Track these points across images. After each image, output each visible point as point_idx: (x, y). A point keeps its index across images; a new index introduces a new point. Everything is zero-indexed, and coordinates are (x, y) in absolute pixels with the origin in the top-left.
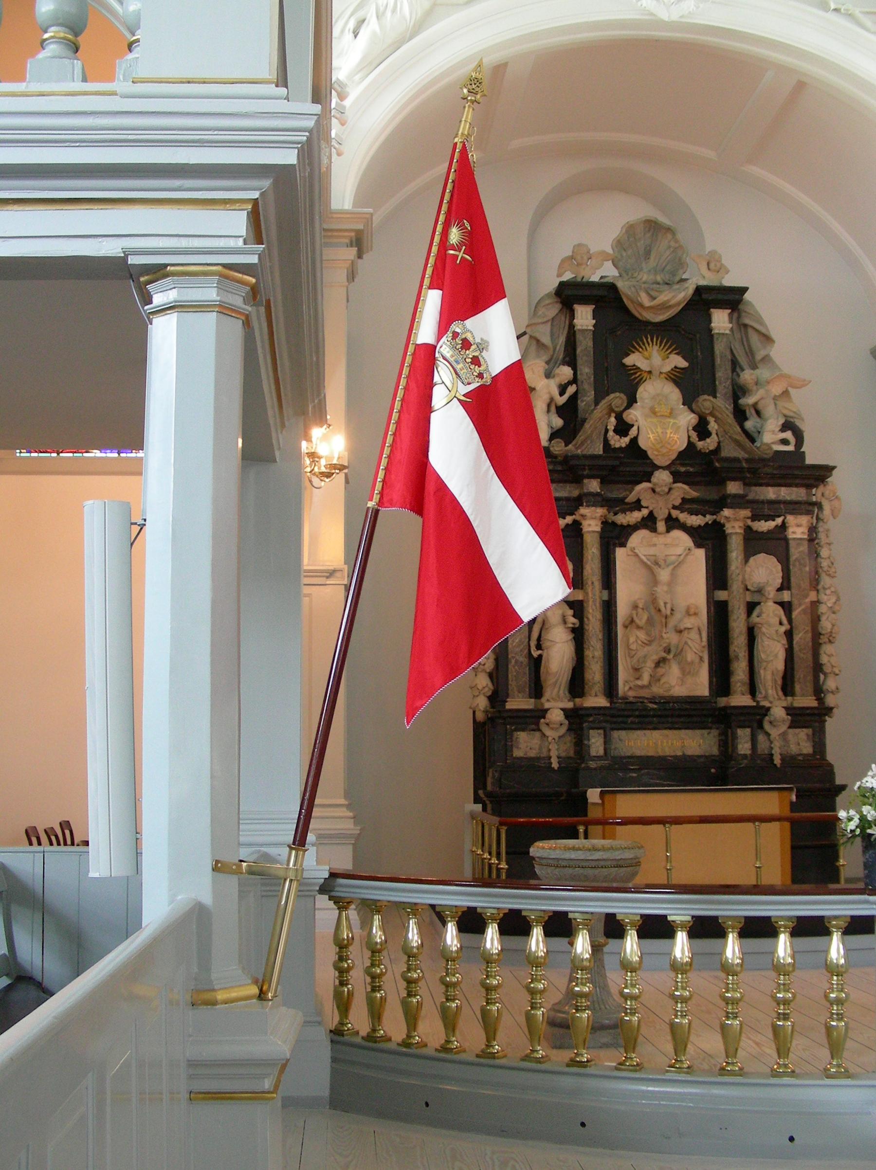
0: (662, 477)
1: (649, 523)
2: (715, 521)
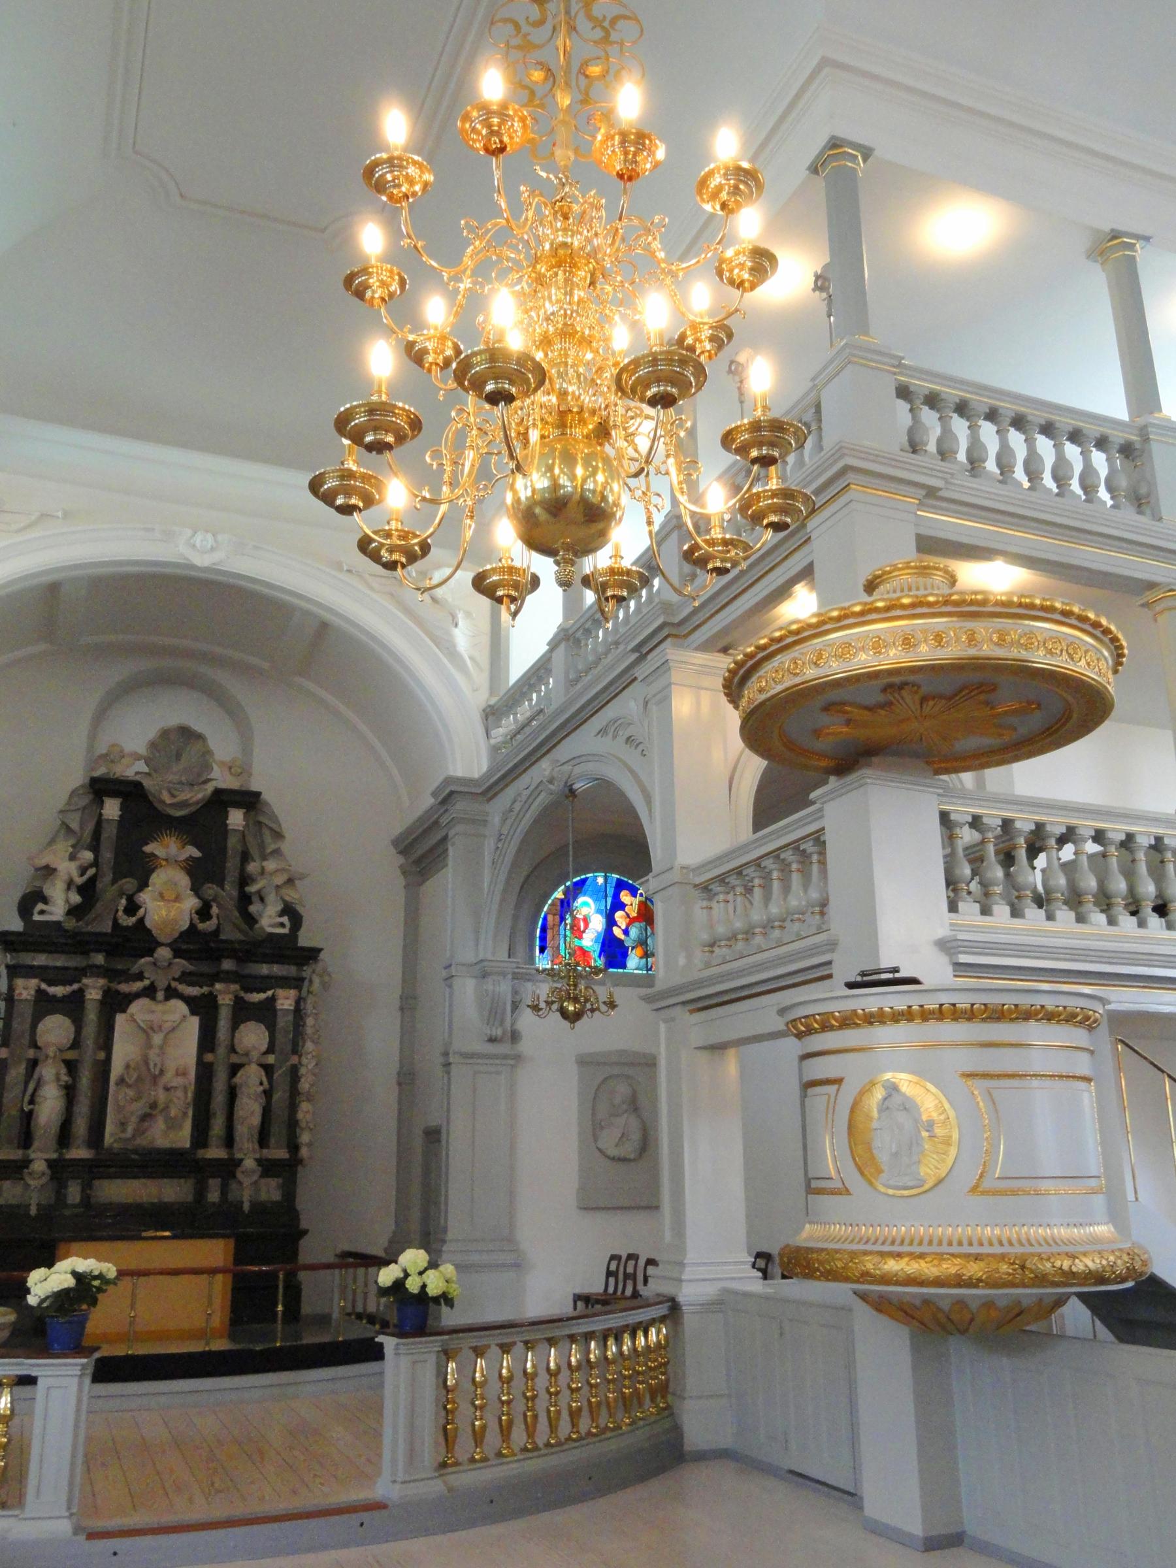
0: (164, 953)
1: (149, 992)
2: (211, 993)
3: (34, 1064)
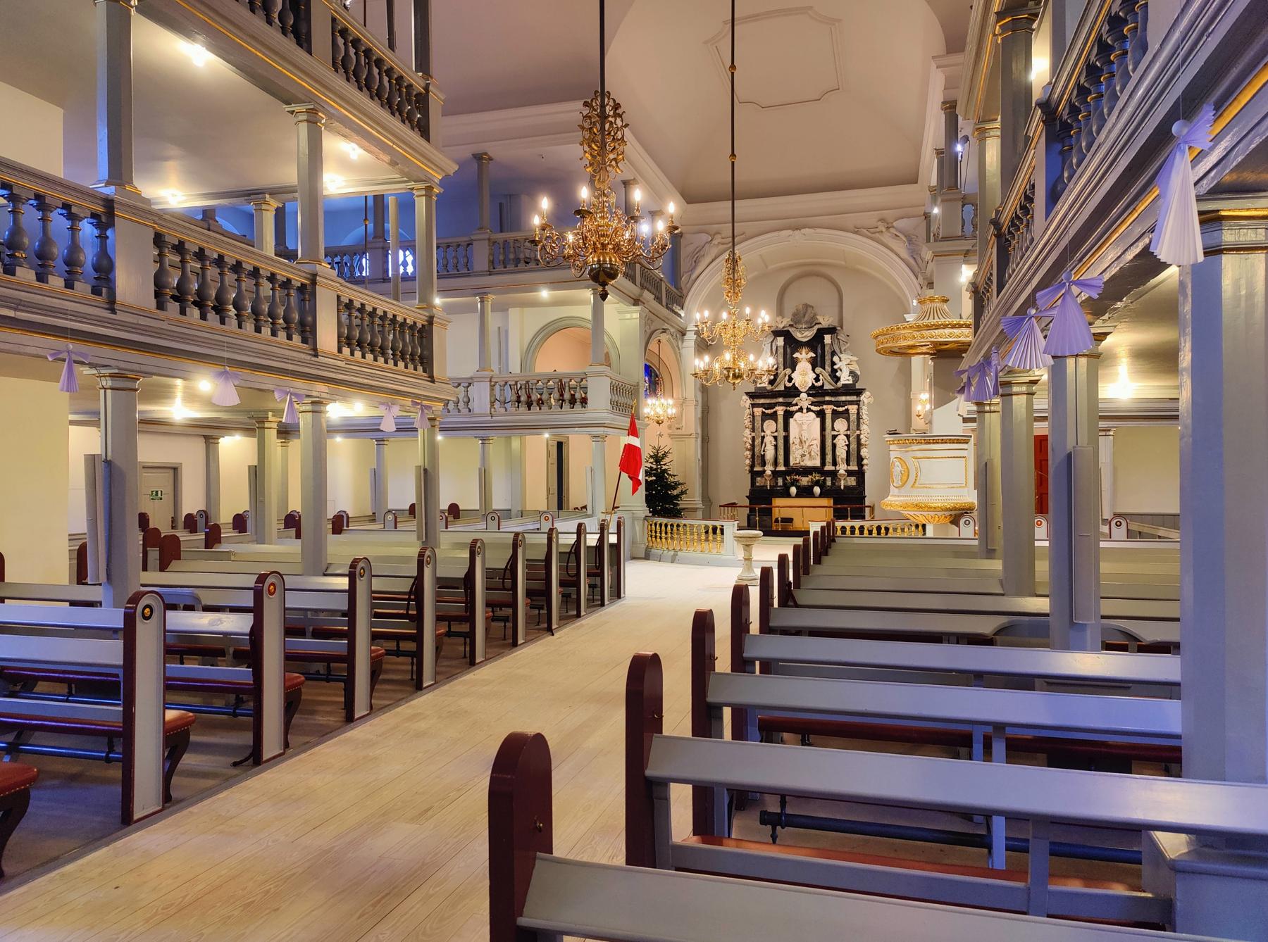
0: (804, 396)
1: (801, 410)
3: (763, 438)
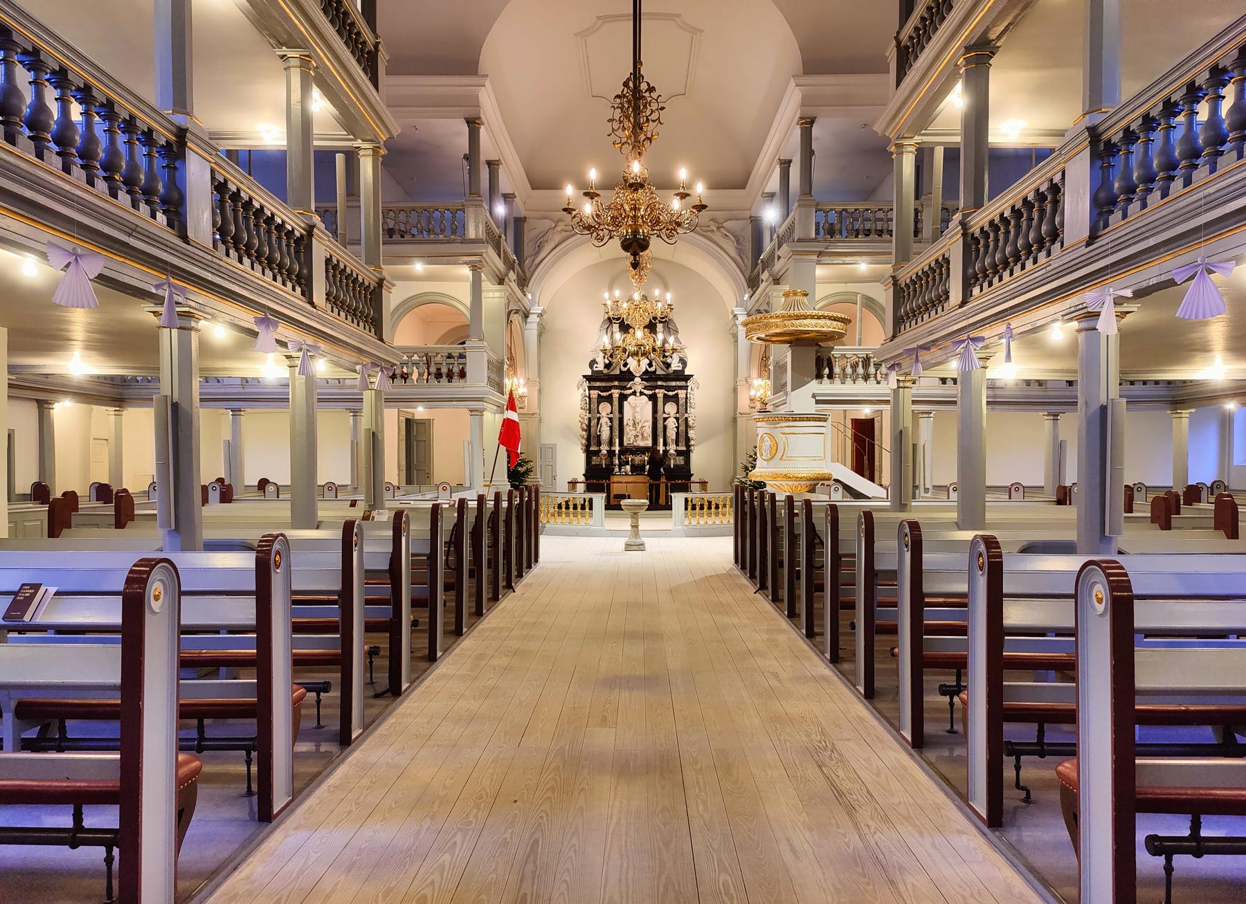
0: (638, 380)
1: (634, 393)
